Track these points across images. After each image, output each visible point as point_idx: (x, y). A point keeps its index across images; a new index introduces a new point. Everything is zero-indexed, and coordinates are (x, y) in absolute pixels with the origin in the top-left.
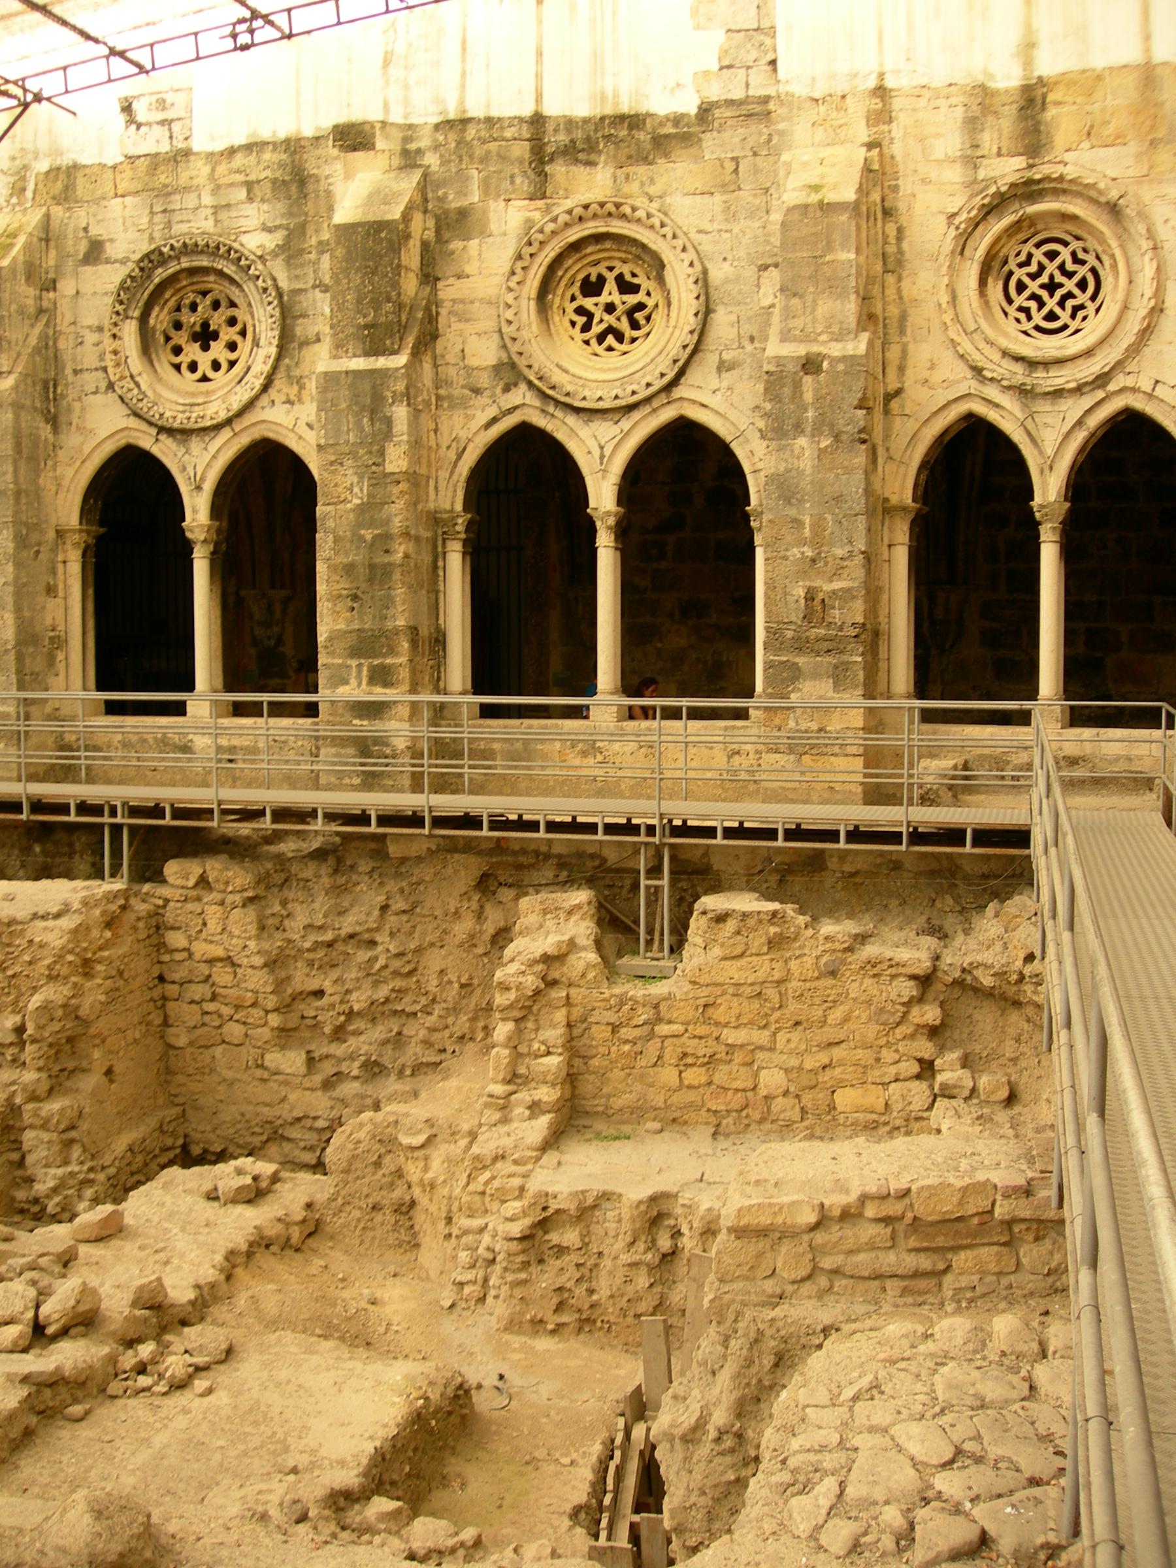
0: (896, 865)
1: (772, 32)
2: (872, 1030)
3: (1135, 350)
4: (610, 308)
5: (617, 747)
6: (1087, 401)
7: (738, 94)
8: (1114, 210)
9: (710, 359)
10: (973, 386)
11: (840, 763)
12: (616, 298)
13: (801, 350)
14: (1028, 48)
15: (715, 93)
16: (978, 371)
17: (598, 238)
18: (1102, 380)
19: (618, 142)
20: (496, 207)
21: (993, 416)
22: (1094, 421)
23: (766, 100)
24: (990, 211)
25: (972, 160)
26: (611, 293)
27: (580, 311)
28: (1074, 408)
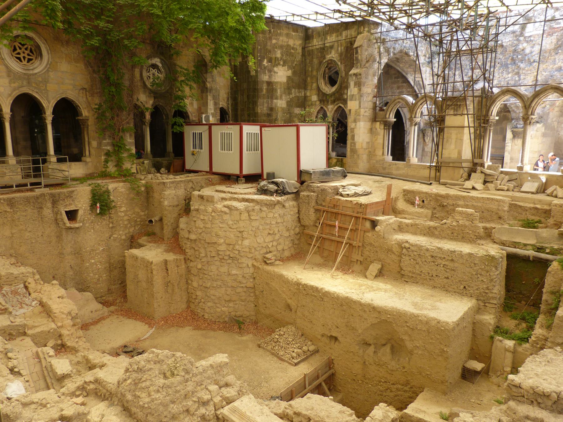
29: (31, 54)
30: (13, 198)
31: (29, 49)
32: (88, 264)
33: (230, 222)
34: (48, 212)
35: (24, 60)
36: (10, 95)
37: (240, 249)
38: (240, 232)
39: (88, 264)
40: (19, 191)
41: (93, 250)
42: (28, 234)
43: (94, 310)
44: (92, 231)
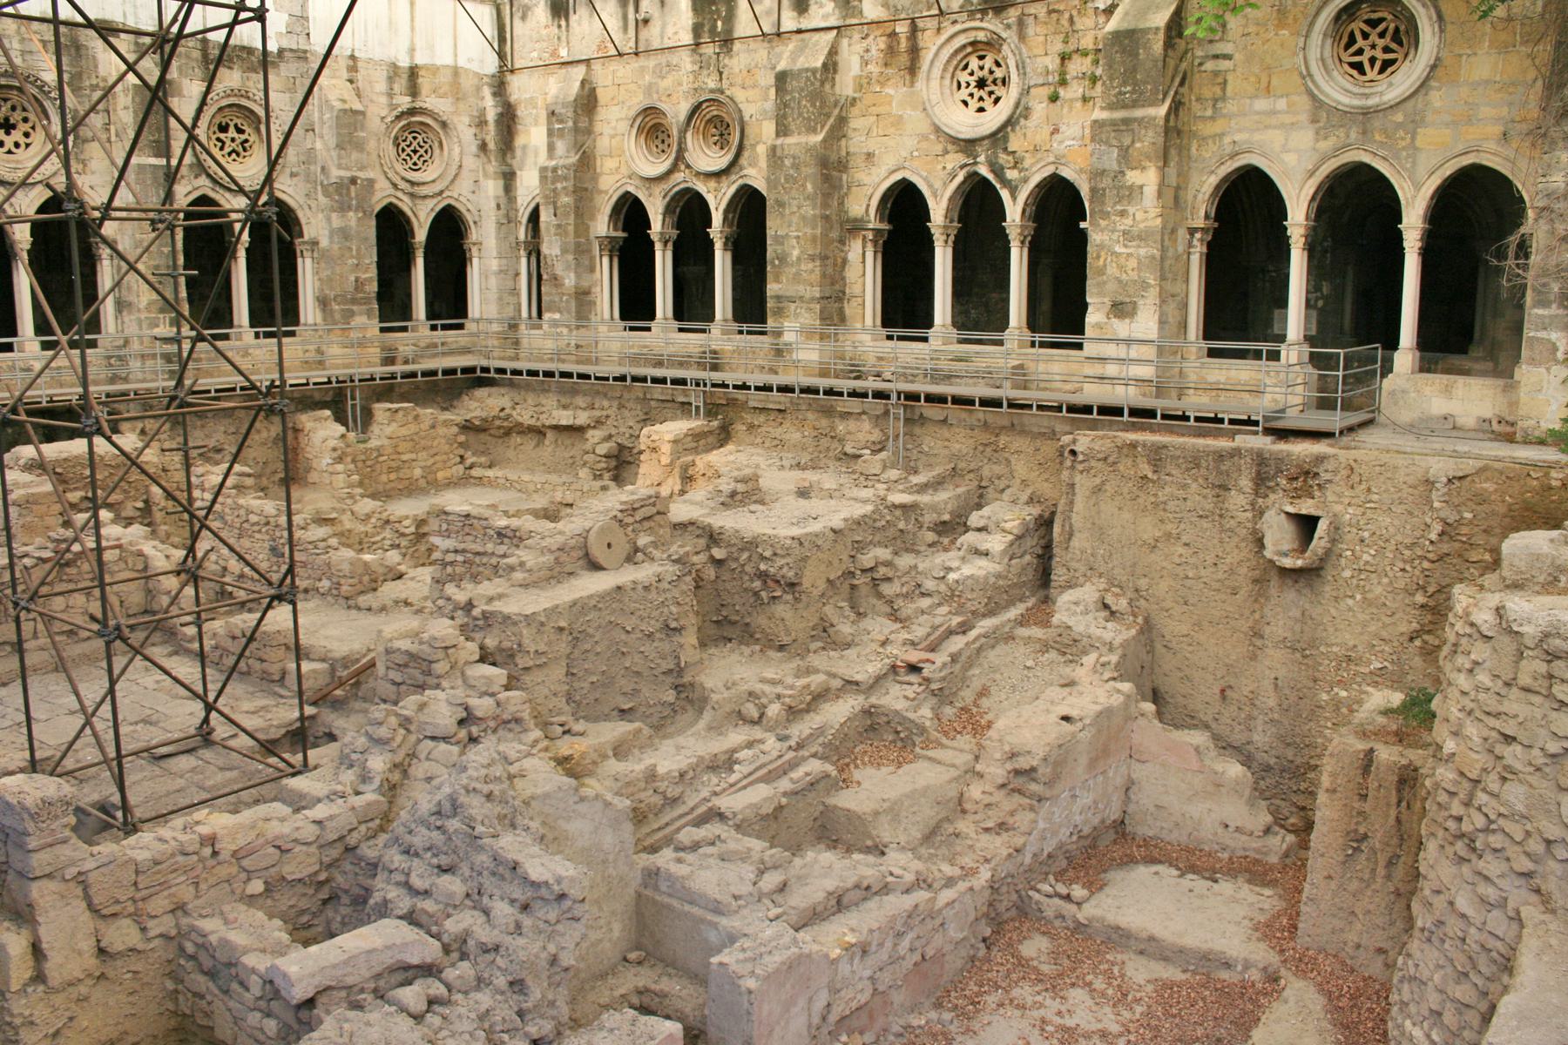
0: (417, 387)
1: (307, 19)
2: (447, 447)
3: (453, 181)
4: (233, 140)
5: (258, 352)
6: (435, 201)
7: (294, 47)
8: (444, 125)
9: (288, 171)
10: (392, 191)
11: (371, 350)
12: (235, 135)
13: (348, 174)
14: (412, 50)
15: (285, 44)
16: (395, 186)
17: (230, 106)
18: (441, 192)
19: (243, 60)
20: (186, 82)
21: (400, 204)
22: (438, 209)
23: (305, 52)
24: (398, 118)
25: (390, 95)
26: (232, 133)
27: (218, 139)
28: (430, 203)
29: (1394, 46)
30: (1165, 447)
31: (1389, 35)
32: (1325, 697)
33: (1483, 678)
34: (1238, 501)
35: (1372, 67)
36: (1312, 174)
37: (1493, 817)
38: (1509, 739)
39: (1325, 697)
40: (1170, 431)
41: (1349, 659)
42: (1181, 550)
43: (1232, 825)
44: (1358, 597)
